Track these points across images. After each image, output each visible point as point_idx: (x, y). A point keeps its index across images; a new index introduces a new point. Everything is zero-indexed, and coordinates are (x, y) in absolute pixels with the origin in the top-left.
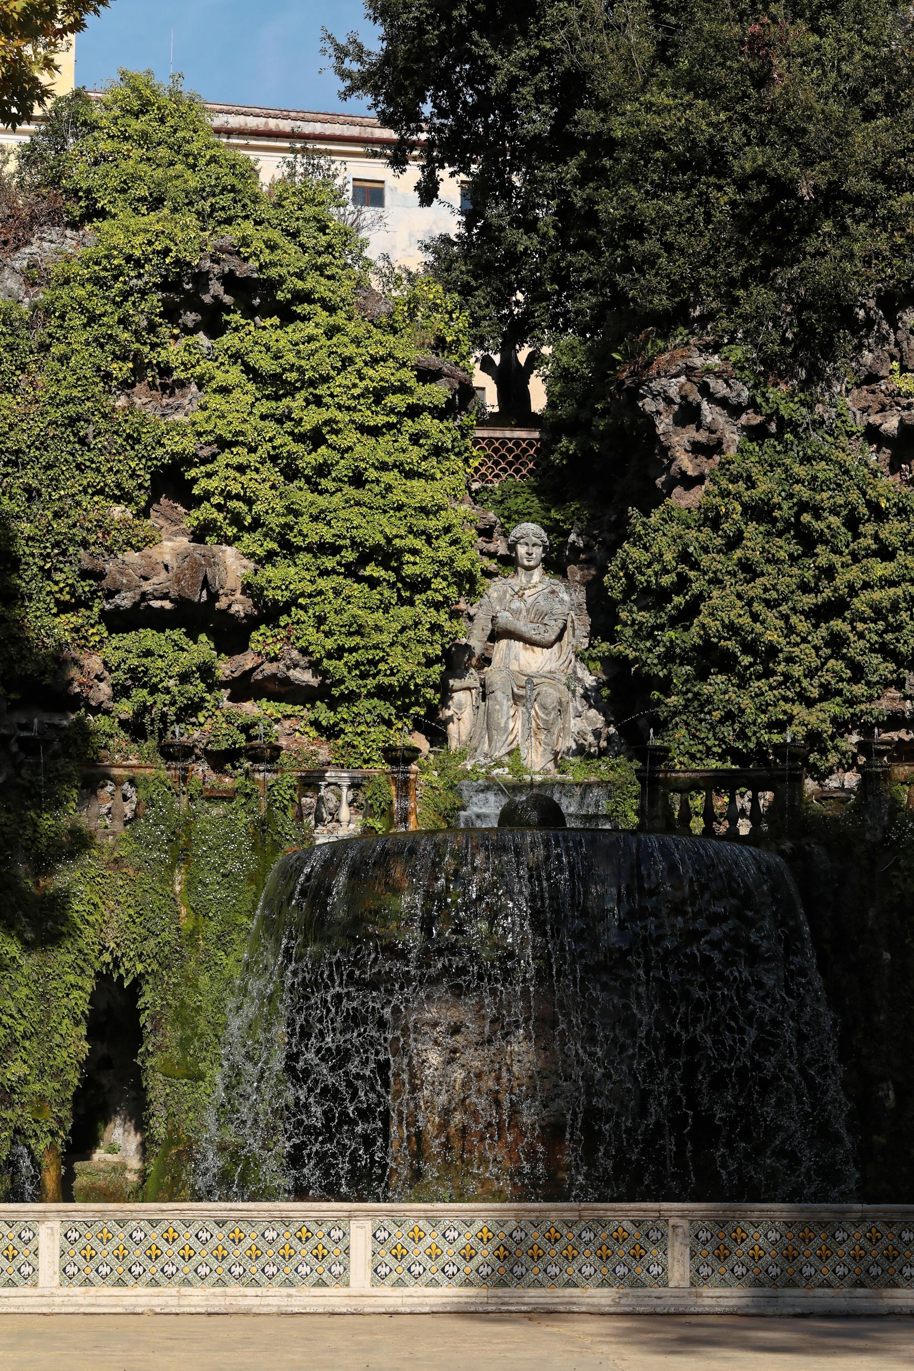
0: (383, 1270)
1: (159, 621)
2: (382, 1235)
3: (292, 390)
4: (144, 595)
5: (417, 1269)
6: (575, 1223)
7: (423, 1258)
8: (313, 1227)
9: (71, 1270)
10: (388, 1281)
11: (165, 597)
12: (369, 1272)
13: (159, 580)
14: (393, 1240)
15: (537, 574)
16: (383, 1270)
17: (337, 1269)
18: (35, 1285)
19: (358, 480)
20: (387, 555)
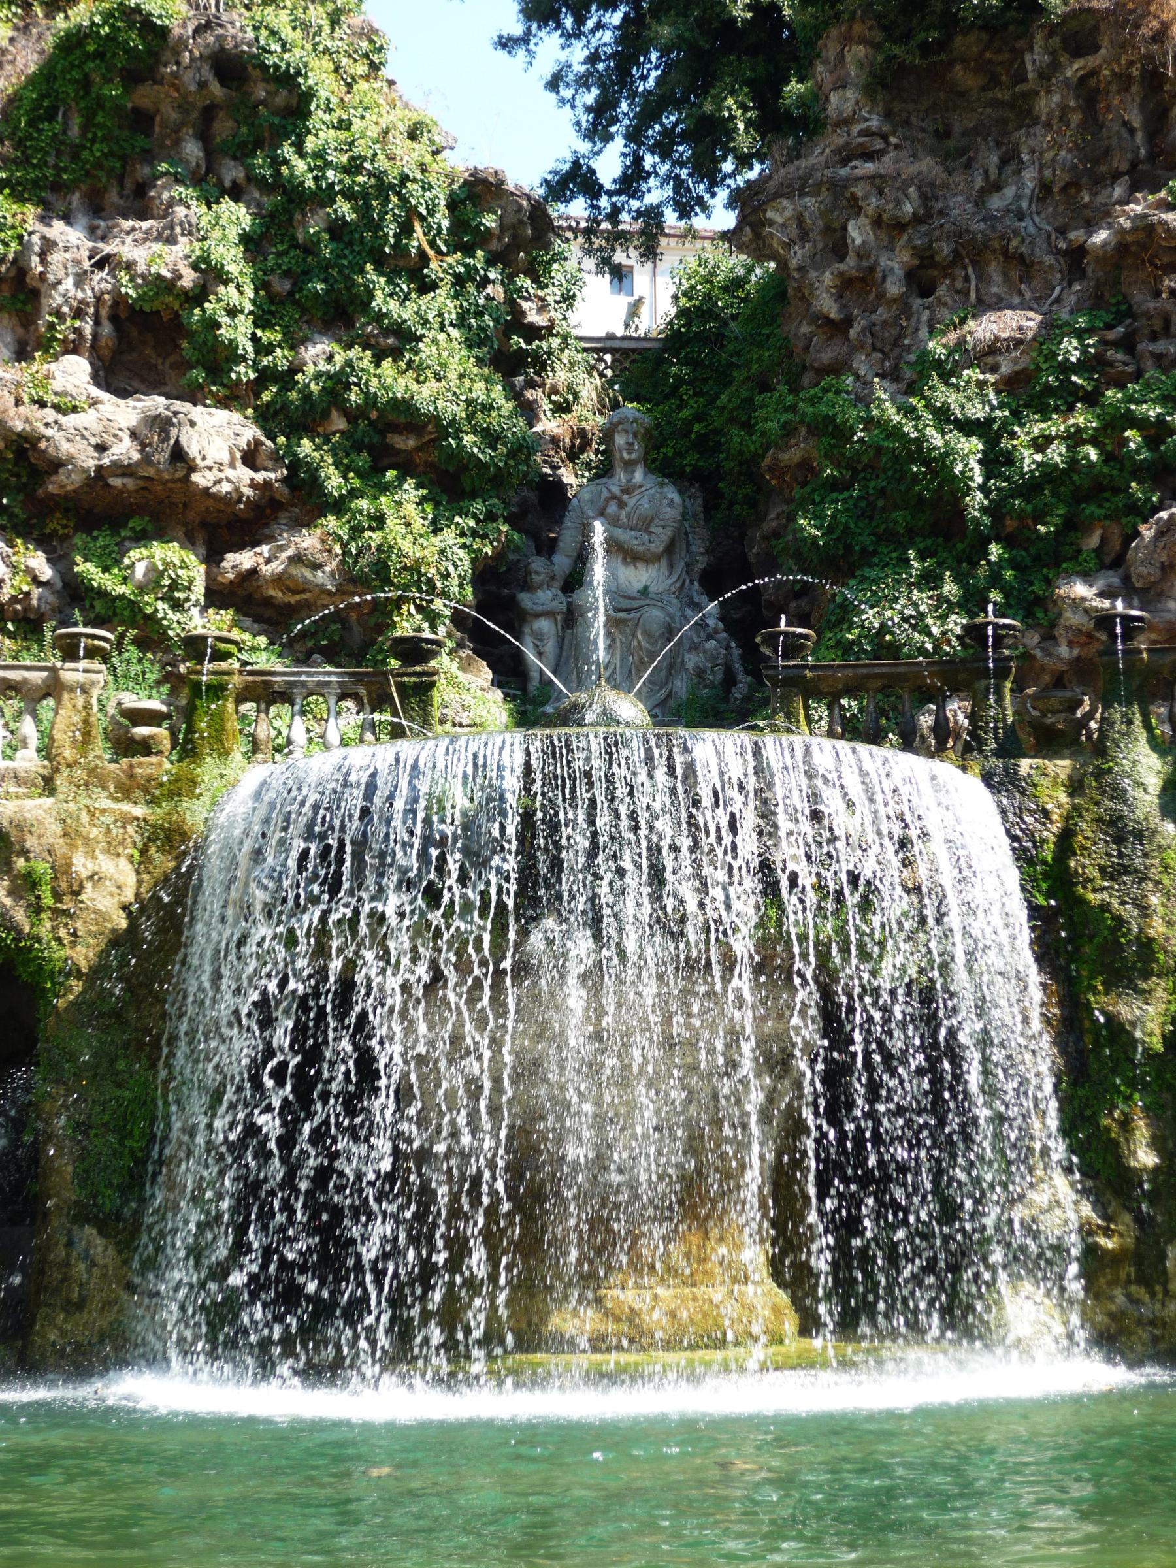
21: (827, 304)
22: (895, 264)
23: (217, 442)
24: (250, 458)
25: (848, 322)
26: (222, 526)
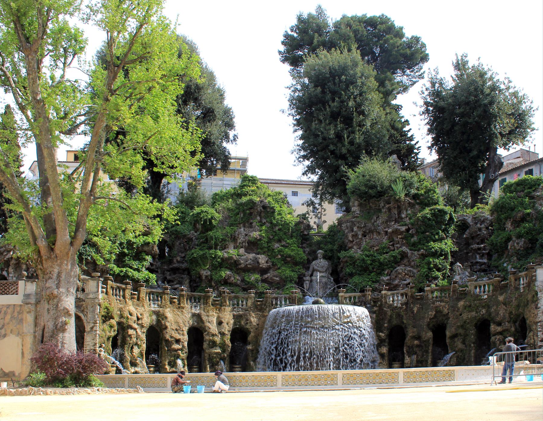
11: (250, 265)
21: (350, 239)
22: (360, 233)
23: (263, 259)
24: (267, 262)
25: (353, 241)
26: (263, 271)
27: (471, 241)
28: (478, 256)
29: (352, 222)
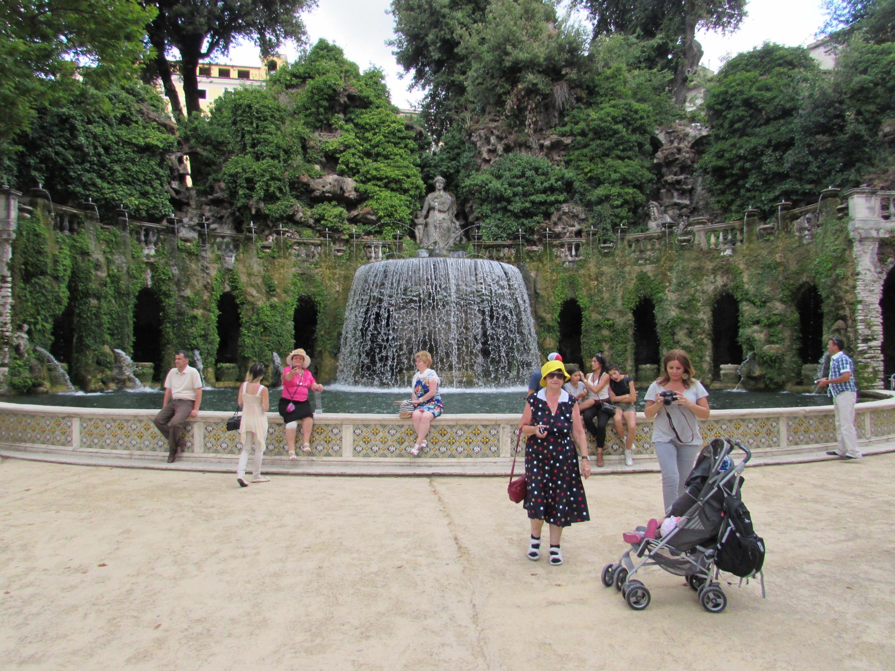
0: (359, 449)
1: (329, 200)
2: (358, 432)
3: (367, 130)
4: (323, 192)
5: (375, 448)
6: (454, 426)
7: (378, 443)
8: (325, 428)
9: (209, 445)
10: (361, 454)
11: (329, 192)
12: (352, 449)
13: (328, 187)
14: (364, 434)
15: (442, 192)
16: (359, 449)
17: (336, 448)
18: (193, 452)
19: (386, 157)
20: (397, 181)
21: (485, 155)
22: (500, 148)
25: (490, 160)
26: (351, 204)
27: (664, 170)
28: (675, 194)
29: (489, 129)
